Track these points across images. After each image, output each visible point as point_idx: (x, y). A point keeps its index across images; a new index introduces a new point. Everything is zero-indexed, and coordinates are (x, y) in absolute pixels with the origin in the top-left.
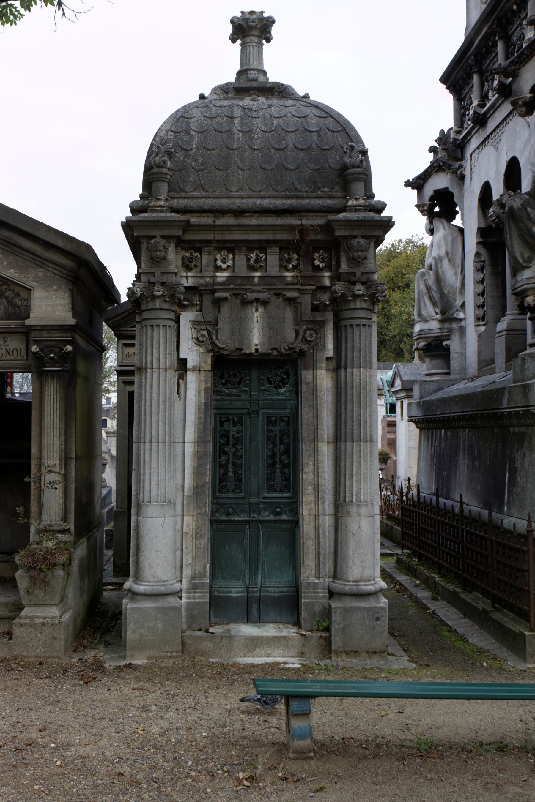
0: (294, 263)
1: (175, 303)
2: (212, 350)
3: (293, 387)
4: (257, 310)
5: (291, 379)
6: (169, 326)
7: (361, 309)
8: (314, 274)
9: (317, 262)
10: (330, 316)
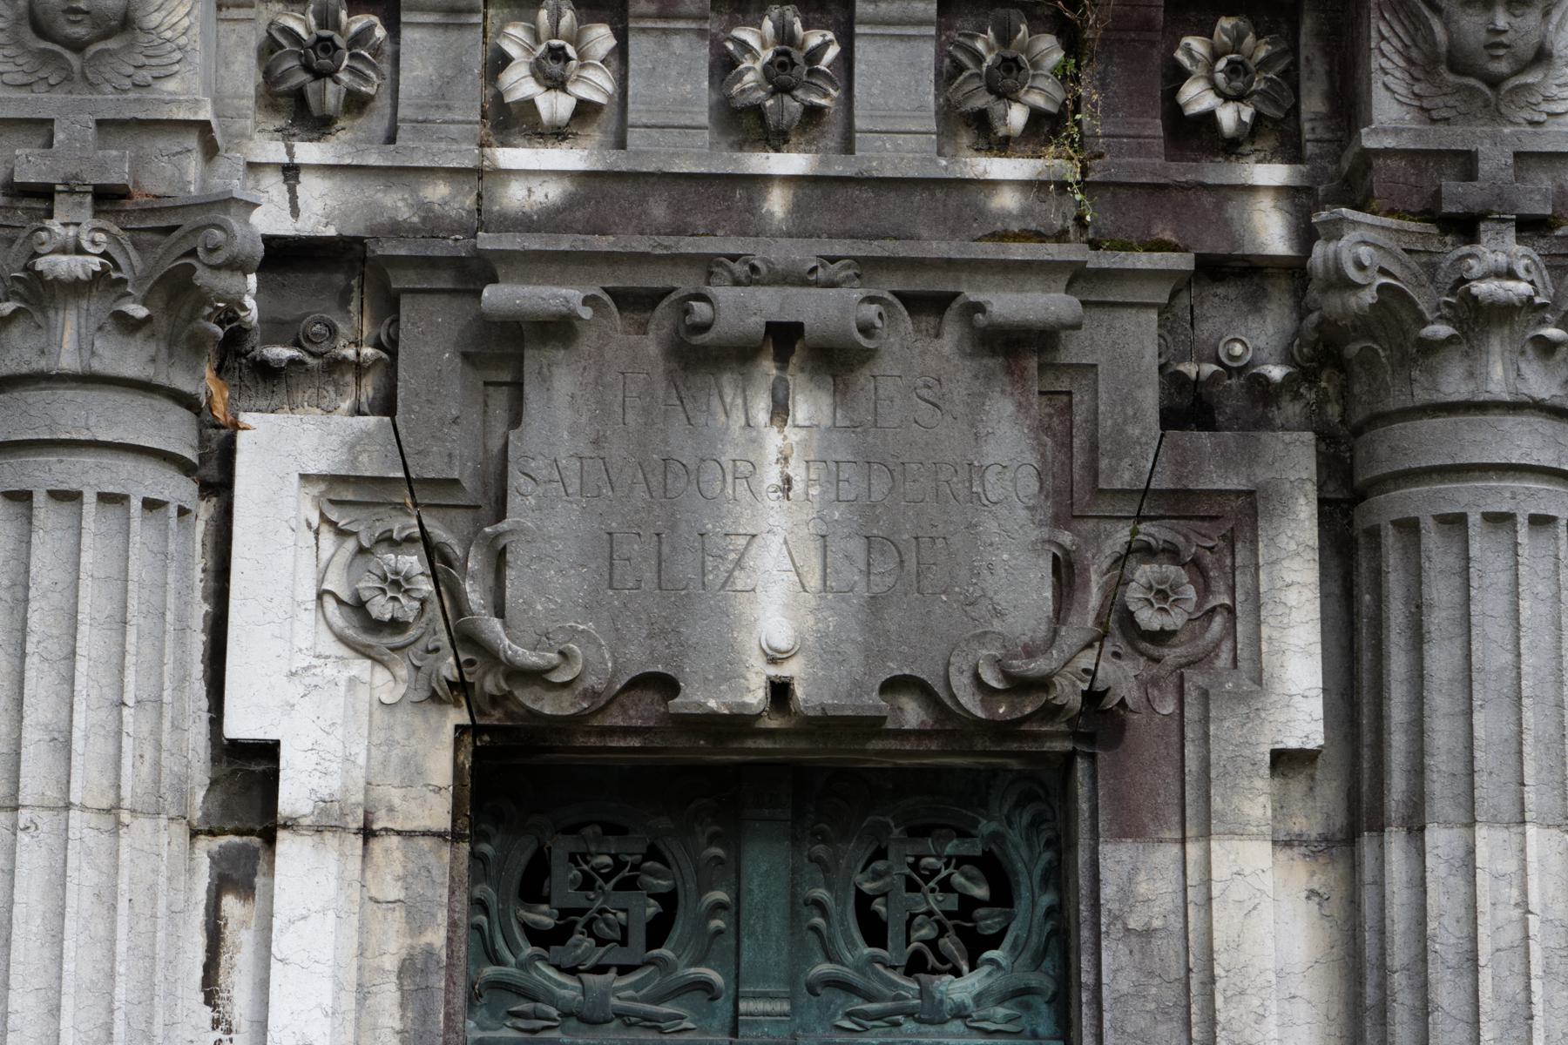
0: (1042, 95)
1: (196, 345)
2: (460, 689)
3: (1037, 961)
4: (780, 411)
5: (1022, 906)
6: (151, 505)
7: (1516, 407)
8: (1180, 172)
9: (1196, 97)
10: (1293, 462)
